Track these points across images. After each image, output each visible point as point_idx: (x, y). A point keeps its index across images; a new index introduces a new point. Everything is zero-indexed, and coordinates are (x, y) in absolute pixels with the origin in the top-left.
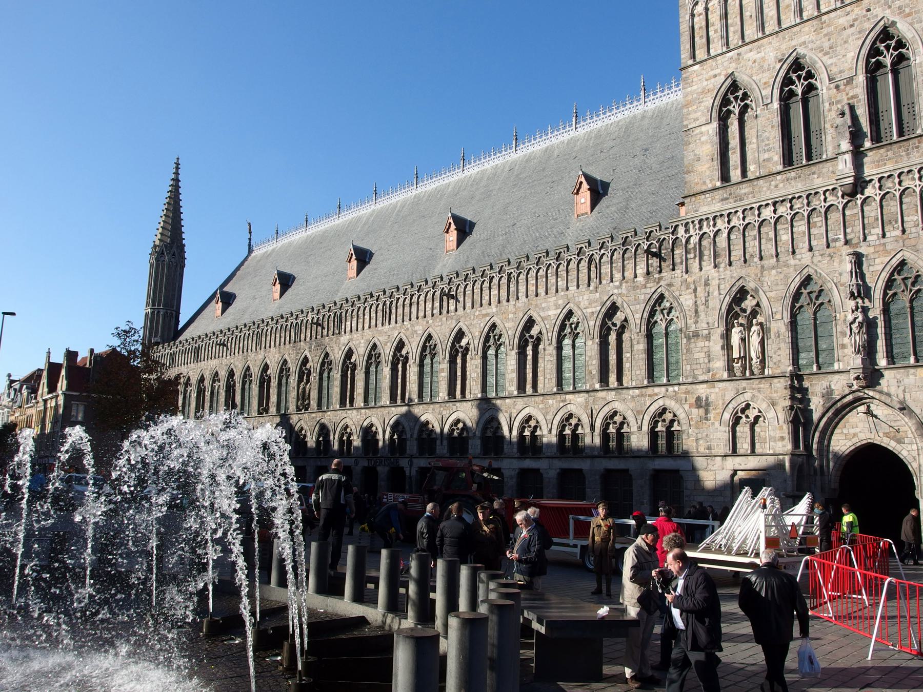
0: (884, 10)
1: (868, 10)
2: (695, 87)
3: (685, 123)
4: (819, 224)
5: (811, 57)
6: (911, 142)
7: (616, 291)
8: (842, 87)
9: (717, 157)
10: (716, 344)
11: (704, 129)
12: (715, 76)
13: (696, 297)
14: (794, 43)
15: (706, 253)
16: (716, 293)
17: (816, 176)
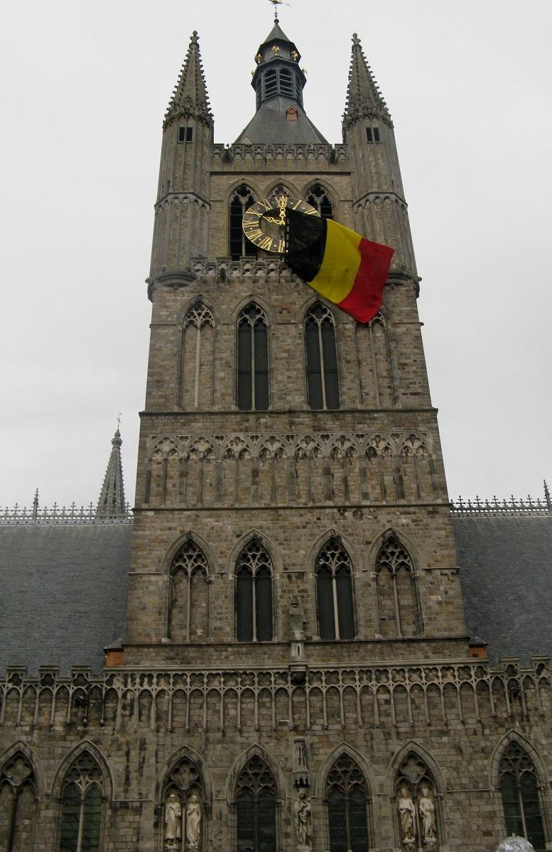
0: (331, 524)
1: (319, 519)
2: (148, 533)
3: (132, 566)
4: (268, 705)
5: (268, 541)
6: (352, 646)
7: (24, 738)
8: (294, 579)
11: (153, 578)
12: (170, 529)
13: (128, 761)
14: (251, 524)
15: (145, 712)
16: (153, 760)
17: (266, 656)
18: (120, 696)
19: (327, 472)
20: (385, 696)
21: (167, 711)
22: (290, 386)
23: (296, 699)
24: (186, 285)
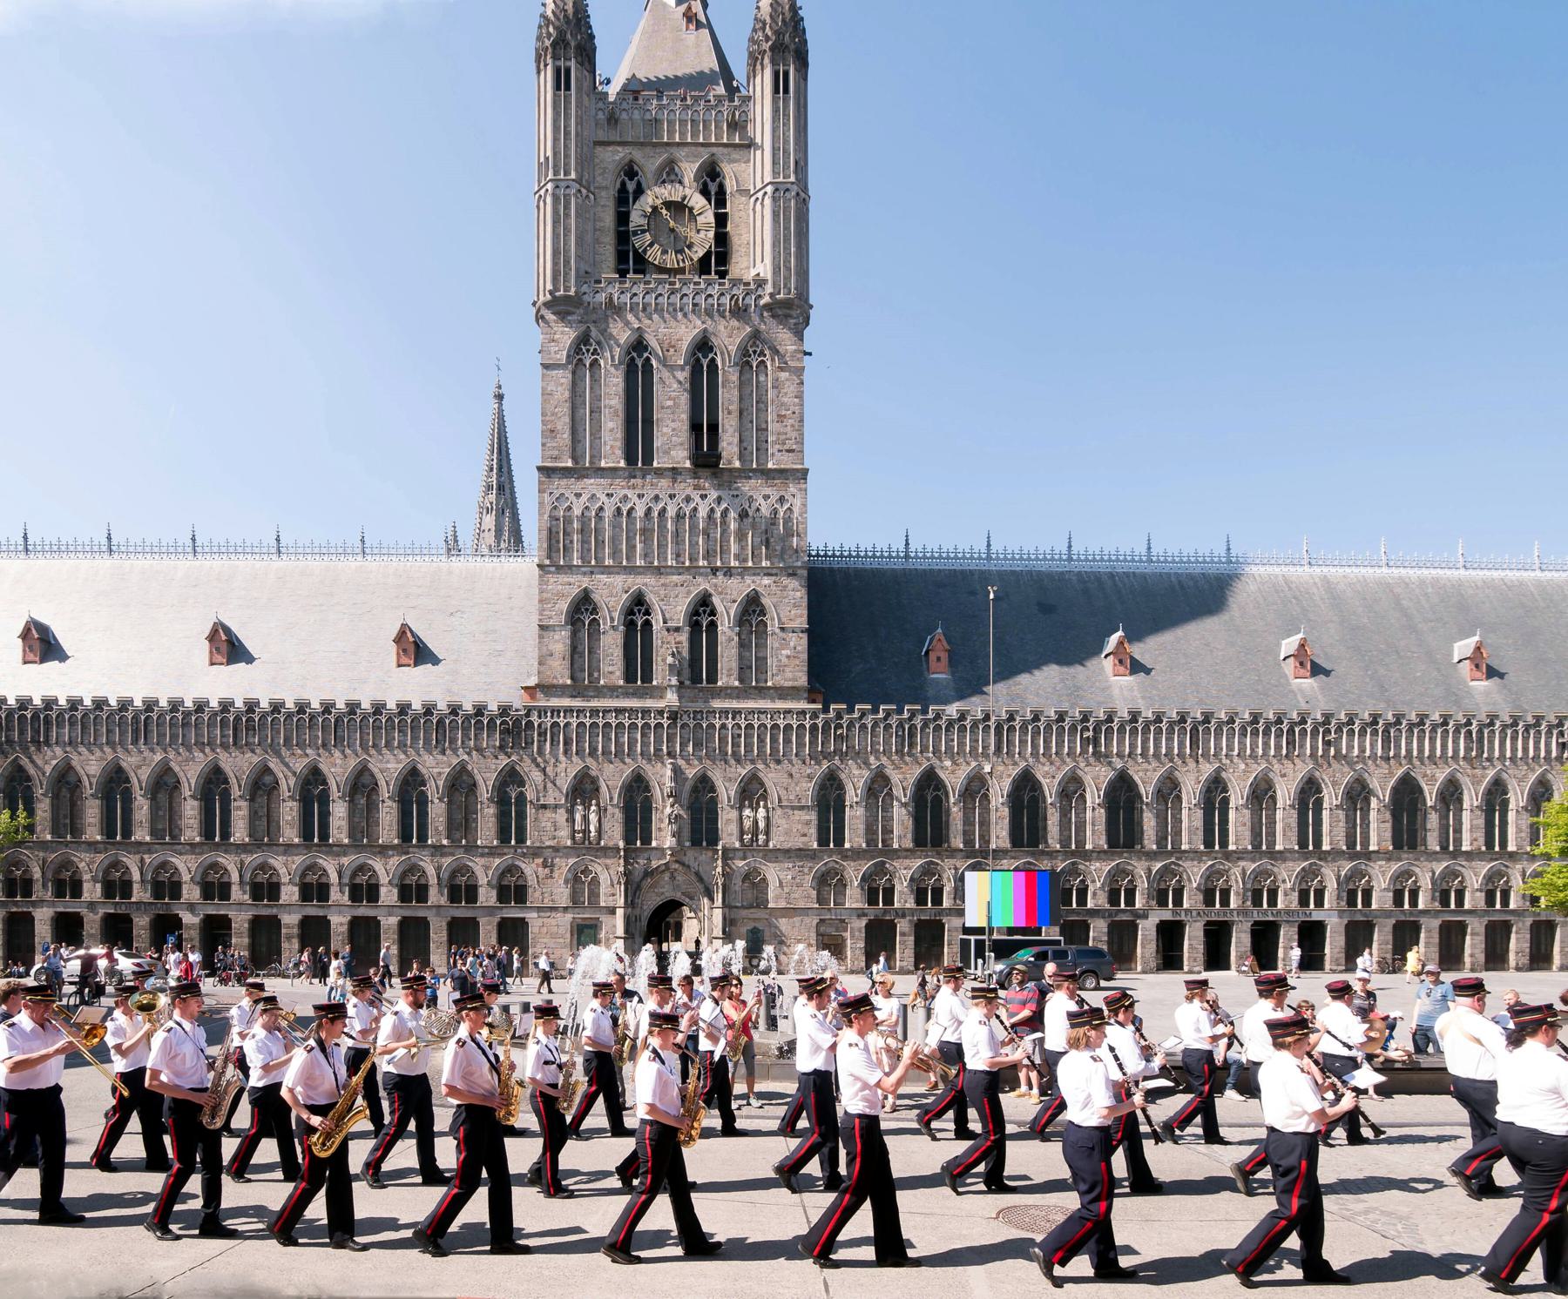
5: (651, 598)
9: (568, 657)
10: (561, 816)
19: (706, 534)
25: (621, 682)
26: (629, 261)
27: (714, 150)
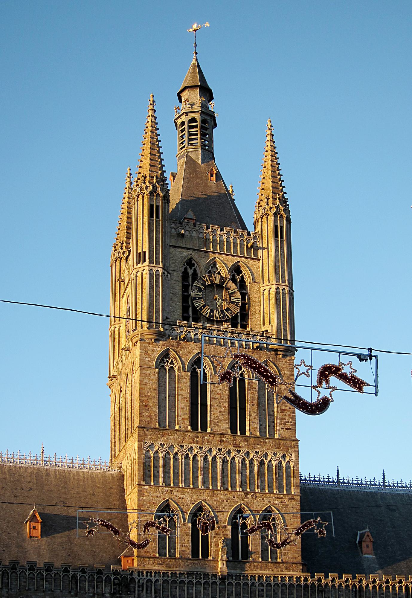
1: (234, 497)
2: (145, 498)
15: (149, 589)
18: (137, 581)
19: (241, 472)
20: (262, 588)
21: (160, 590)
22: (221, 417)
23: (221, 587)
24: (160, 340)
25: (190, 557)
26: (191, 313)
27: (239, 259)
